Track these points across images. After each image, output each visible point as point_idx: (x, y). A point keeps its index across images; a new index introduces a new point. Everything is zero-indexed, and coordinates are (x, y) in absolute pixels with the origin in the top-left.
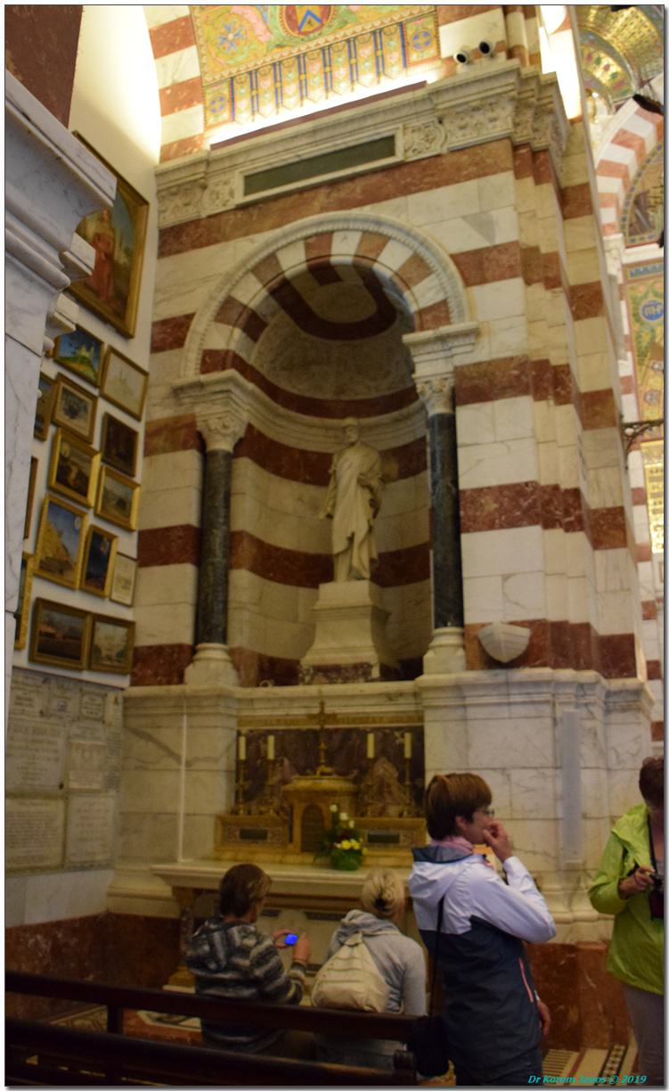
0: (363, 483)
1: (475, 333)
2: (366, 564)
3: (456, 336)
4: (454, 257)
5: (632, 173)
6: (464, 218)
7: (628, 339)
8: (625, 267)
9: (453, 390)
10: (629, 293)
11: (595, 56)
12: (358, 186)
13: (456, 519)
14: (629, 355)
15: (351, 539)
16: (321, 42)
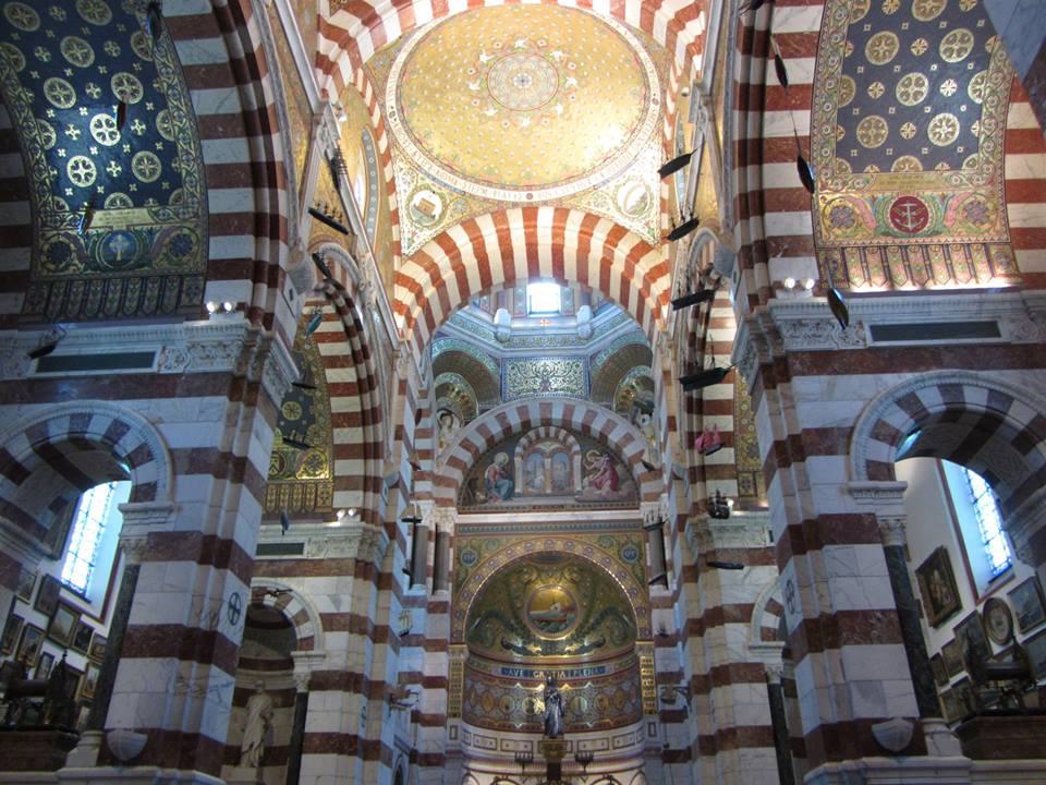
0: (263, 716)
1: (324, 656)
2: (257, 757)
3: (315, 656)
4: (321, 615)
5: (469, 466)
6: (329, 595)
7: (450, 573)
8: (456, 525)
9: (310, 682)
10: (455, 541)
11: (456, 390)
12: (283, 565)
13: (301, 746)
14: (450, 585)
15: (252, 746)
16: (278, 482)
